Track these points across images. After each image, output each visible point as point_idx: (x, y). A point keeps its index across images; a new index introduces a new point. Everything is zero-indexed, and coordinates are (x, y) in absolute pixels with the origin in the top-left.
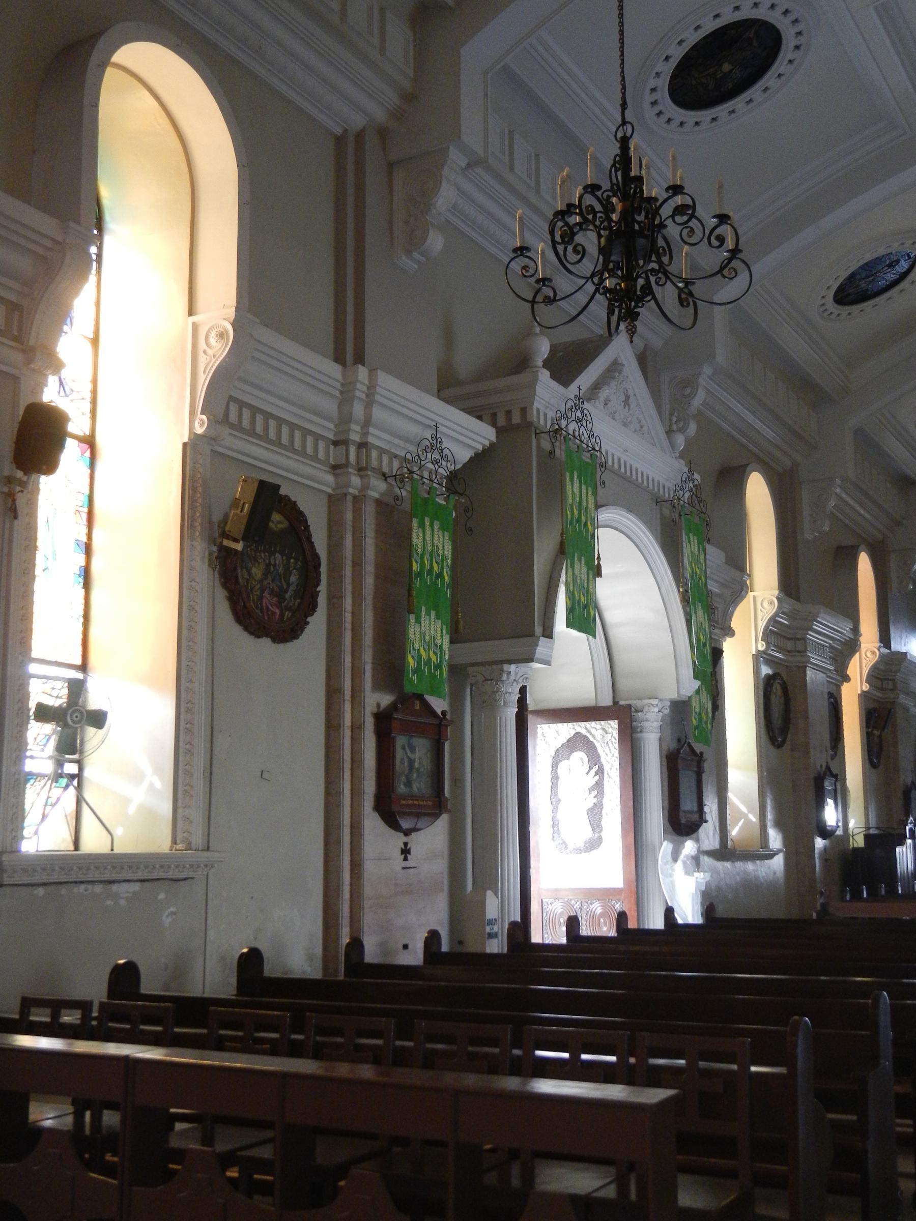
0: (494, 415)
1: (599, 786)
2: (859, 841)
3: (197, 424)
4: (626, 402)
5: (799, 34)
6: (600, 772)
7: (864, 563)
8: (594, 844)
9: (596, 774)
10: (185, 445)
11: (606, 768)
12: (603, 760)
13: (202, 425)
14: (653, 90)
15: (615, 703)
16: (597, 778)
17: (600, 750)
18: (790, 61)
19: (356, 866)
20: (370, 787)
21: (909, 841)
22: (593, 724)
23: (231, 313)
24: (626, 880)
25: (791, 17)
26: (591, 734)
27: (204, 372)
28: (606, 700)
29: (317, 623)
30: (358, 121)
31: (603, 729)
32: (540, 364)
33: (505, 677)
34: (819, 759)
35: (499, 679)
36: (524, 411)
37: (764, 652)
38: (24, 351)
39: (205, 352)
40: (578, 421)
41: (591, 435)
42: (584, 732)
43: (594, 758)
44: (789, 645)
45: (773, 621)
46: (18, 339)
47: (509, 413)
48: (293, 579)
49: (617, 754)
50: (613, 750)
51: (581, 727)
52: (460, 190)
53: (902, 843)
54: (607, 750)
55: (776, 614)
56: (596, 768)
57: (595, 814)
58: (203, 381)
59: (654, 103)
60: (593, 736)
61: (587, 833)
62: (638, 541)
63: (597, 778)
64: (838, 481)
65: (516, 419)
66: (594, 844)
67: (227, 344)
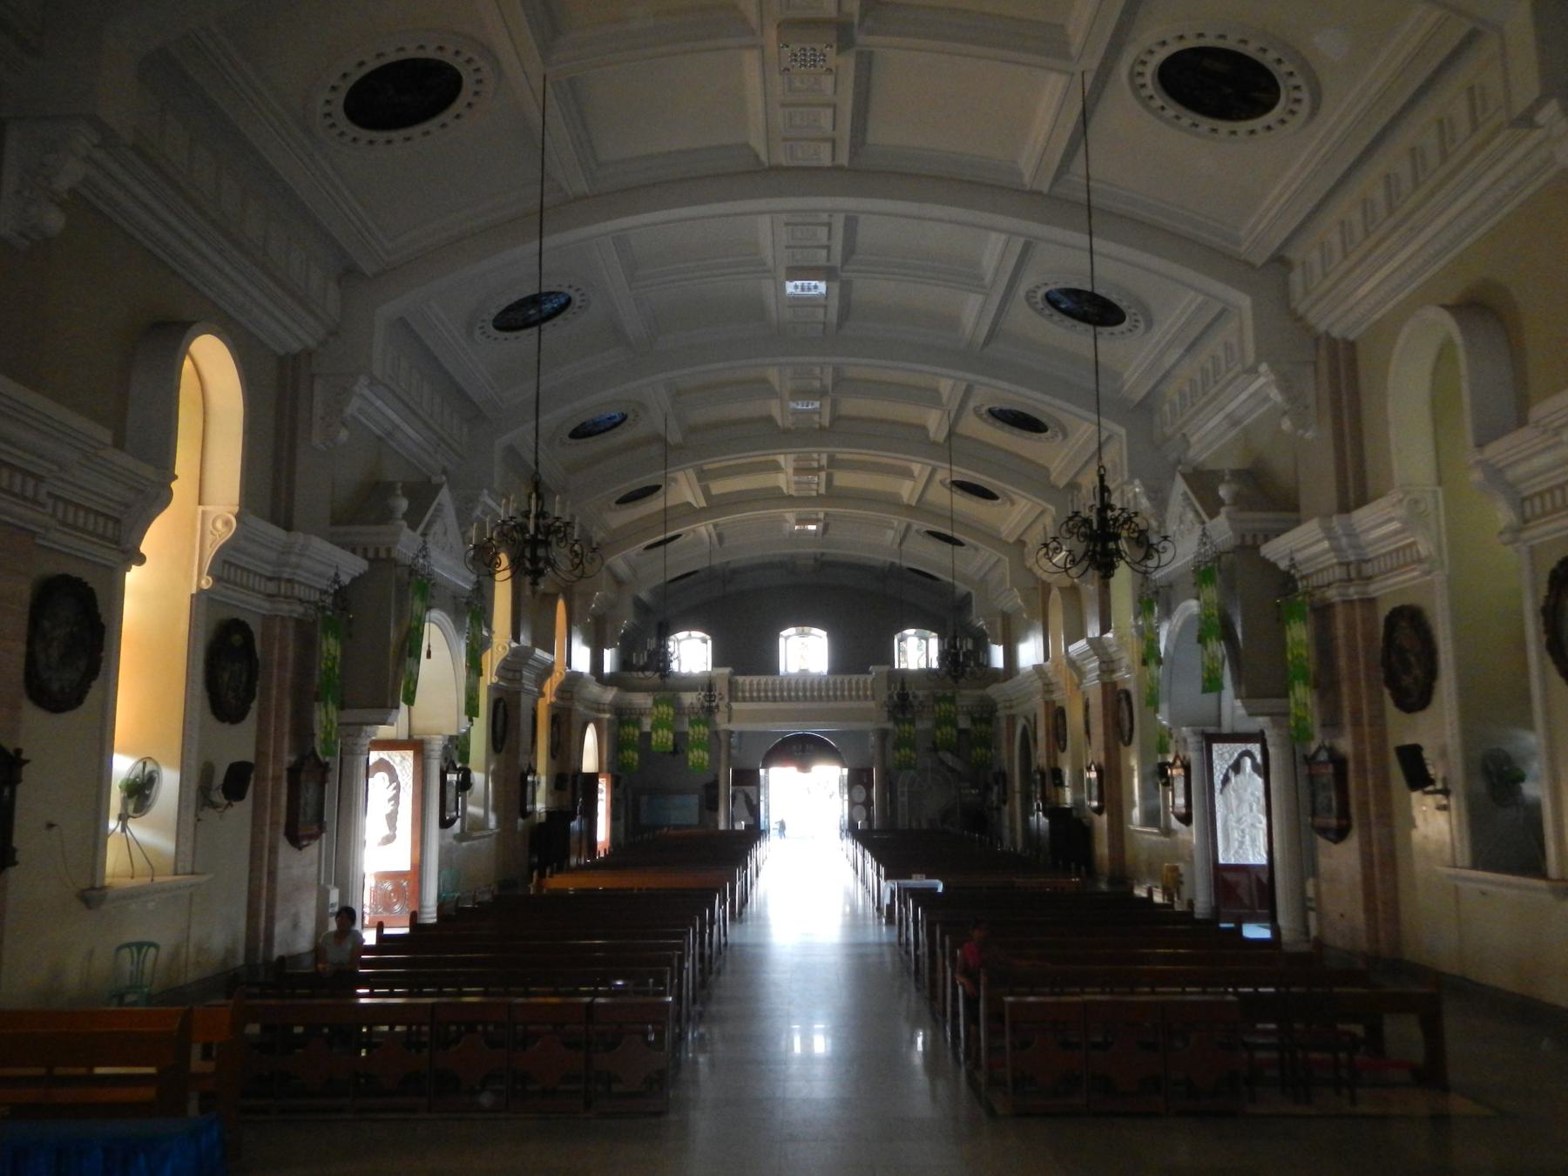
0: (365, 550)
1: (396, 799)
2: (543, 818)
3: (203, 582)
4: (445, 533)
5: (583, 301)
6: (398, 788)
7: (561, 606)
8: (389, 840)
9: (394, 789)
11: (402, 785)
12: (400, 779)
13: (208, 582)
14: (484, 321)
15: (410, 736)
16: (395, 791)
17: (398, 772)
19: (272, 875)
20: (283, 820)
21: (578, 817)
22: (394, 752)
23: (236, 509)
24: (413, 865)
25: (580, 292)
26: (391, 759)
27: (211, 546)
28: (403, 735)
29: (254, 705)
30: (296, 347)
32: (400, 516)
33: (363, 734)
34: (523, 761)
35: (359, 736)
36: (389, 551)
37: (497, 683)
38: (123, 552)
39: (212, 533)
40: (424, 557)
42: (387, 758)
43: (393, 777)
44: (510, 675)
45: (505, 660)
46: (117, 543)
47: (377, 551)
49: (411, 775)
51: (384, 755)
53: (574, 819)
54: (404, 772)
55: (507, 656)
57: (392, 819)
58: (210, 553)
59: (482, 328)
60: (394, 762)
61: (386, 831)
63: (395, 791)
65: (383, 554)
66: (389, 840)
67: (230, 530)
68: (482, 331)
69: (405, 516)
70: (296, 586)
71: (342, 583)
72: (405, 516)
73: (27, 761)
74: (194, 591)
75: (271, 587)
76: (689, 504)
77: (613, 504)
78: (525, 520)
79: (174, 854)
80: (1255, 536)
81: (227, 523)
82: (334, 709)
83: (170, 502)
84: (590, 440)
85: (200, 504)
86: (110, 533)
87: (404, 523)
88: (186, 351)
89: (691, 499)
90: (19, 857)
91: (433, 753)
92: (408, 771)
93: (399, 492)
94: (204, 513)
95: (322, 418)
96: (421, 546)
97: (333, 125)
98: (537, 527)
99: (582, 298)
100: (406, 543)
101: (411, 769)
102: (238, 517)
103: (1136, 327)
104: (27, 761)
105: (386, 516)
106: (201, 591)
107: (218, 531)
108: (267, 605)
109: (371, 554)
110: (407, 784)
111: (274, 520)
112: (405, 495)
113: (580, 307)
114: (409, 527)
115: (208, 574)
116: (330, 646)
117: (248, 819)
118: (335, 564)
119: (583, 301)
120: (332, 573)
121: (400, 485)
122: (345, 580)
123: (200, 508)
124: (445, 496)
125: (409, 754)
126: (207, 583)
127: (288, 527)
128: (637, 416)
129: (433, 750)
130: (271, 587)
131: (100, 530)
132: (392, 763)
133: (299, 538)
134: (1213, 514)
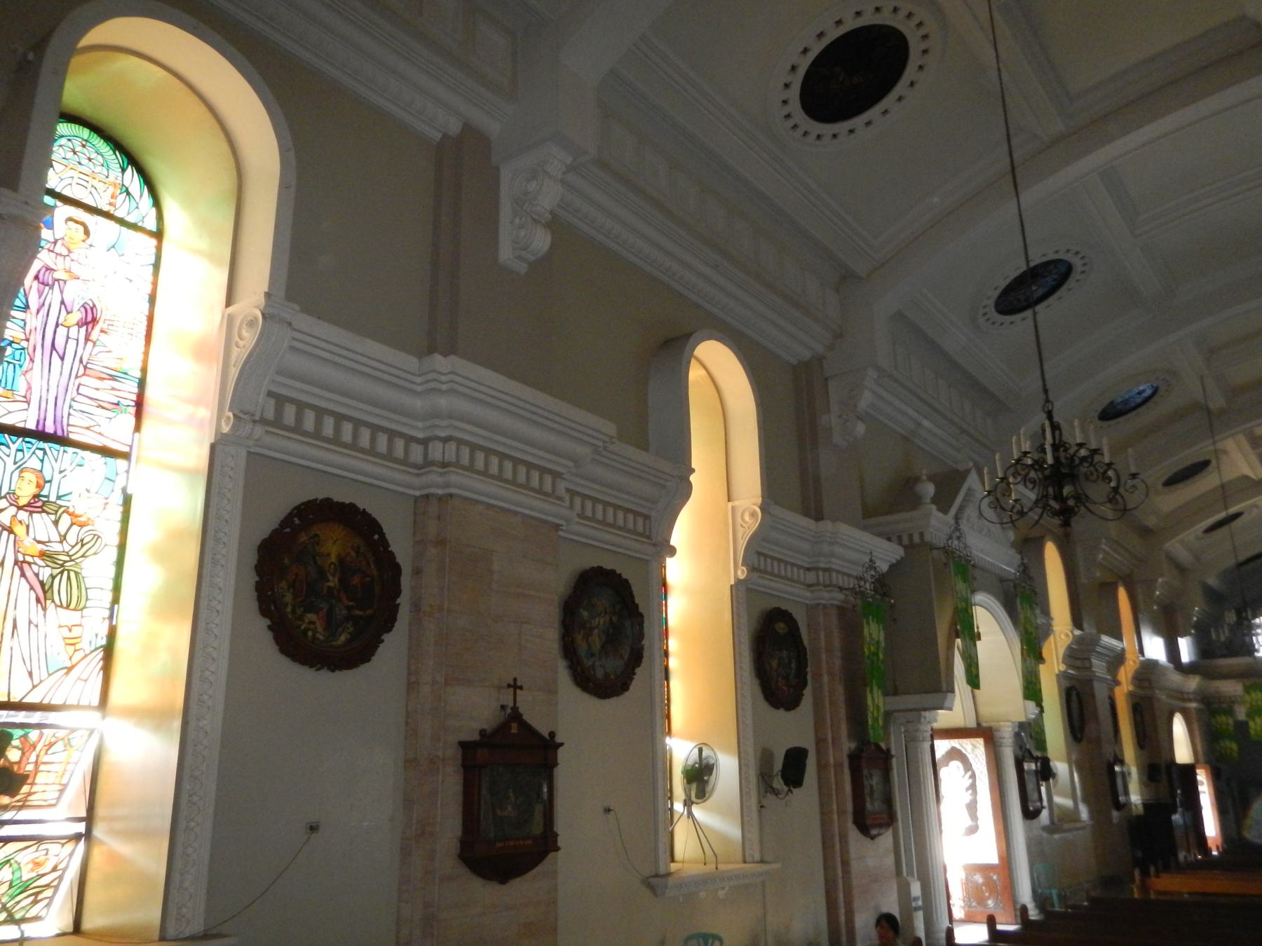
0: (900, 538)
1: (973, 787)
2: (1140, 810)
3: (739, 573)
6: (973, 776)
7: (1122, 594)
8: (973, 830)
10: (731, 586)
14: (985, 307)
15: (979, 724)
16: (971, 781)
18: (1078, 281)
19: (846, 864)
20: (849, 806)
21: (1180, 810)
23: (759, 500)
24: (1000, 857)
25: (1080, 256)
26: (962, 747)
28: (972, 723)
29: (808, 693)
30: (807, 355)
31: (973, 745)
32: (929, 501)
33: (923, 720)
34: (1108, 751)
35: (919, 721)
36: (922, 534)
38: (655, 545)
39: (742, 526)
40: (958, 538)
41: (966, 547)
42: (958, 747)
43: (967, 766)
44: (1079, 663)
45: (1069, 648)
46: (649, 537)
47: (911, 536)
48: (793, 666)
50: (981, 760)
51: (955, 743)
52: (874, 393)
53: (1175, 812)
54: (977, 760)
55: (1072, 643)
56: (969, 773)
57: (972, 808)
58: (742, 545)
59: (985, 314)
60: (965, 749)
61: (968, 822)
62: (992, 611)
64: (1104, 541)
65: (916, 539)
66: (973, 830)
67: (757, 521)
68: (986, 318)
69: (935, 500)
70: (834, 575)
71: (878, 569)
72: (935, 500)
73: (562, 744)
74: (733, 583)
75: (811, 577)
76: (1247, 477)
77: (1160, 487)
78: (1042, 455)
79: (741, 841)
81: (753, 514)
82: (880, 694)
83: (690, 496)
84: (1121, 419)
85: (729, 501)
86: (640, 528)
87: (934, 507)
88: (691, 355)
89: (1247, 471)
91: (1004, 741)
92: (981, 760)
94: (733, 508)
95: (840, 416)
96: (953, 528)
97: (795, 127)
98: (1056, 459)
99: (1084, 262)
100: (937, 525)
101: (984, 757)
102: (762, 508)
104: (562, 744)
105: (915, 502)
106: (739, 582)
107: (746, 523)
108: (808, 594)
109: (906, 541)
110: (982, 772)
111: (806, 513)
113: (1083, 272)
114: (939, 510)
115: (742, 565)
116: (873, 631)
117: (815, 810)
118: (869, 551)
119: (1085, 265)
122: (884, 567)
123: (730, 504)
125: (980, 742)
126: (742, 573)
127: (819, 517)
128: (1169, 386)
129: (1004, 738)
130: (811, 577)
131: (631, 526)
132: (964, 751)
133: (827, 526)
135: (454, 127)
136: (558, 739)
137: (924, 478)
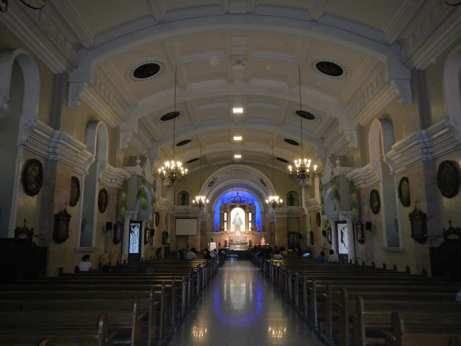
36: (135, 173)
47: (132, 173)
69: (140, 164)
72: (140, 164)
80: (343, 173)
87: (140, 166)
90: (69, 236)
93: (138, 158)
97: (131, 78)
103: (318, 120)
109: (131, 173)
112: (140, 159)
116: (124, 195)
120: (124, 178)
121: (138, 157)
124: (148, 160)
134: (335, 167)
135: (116, 126)
136: (71, 216)
137: (138, 158)
